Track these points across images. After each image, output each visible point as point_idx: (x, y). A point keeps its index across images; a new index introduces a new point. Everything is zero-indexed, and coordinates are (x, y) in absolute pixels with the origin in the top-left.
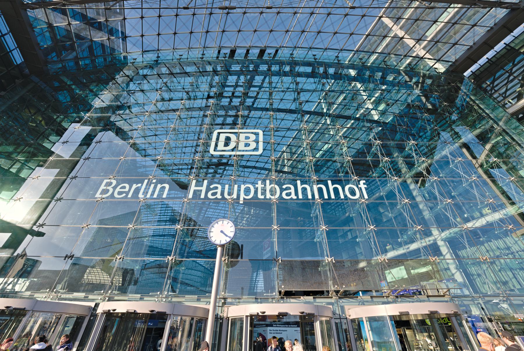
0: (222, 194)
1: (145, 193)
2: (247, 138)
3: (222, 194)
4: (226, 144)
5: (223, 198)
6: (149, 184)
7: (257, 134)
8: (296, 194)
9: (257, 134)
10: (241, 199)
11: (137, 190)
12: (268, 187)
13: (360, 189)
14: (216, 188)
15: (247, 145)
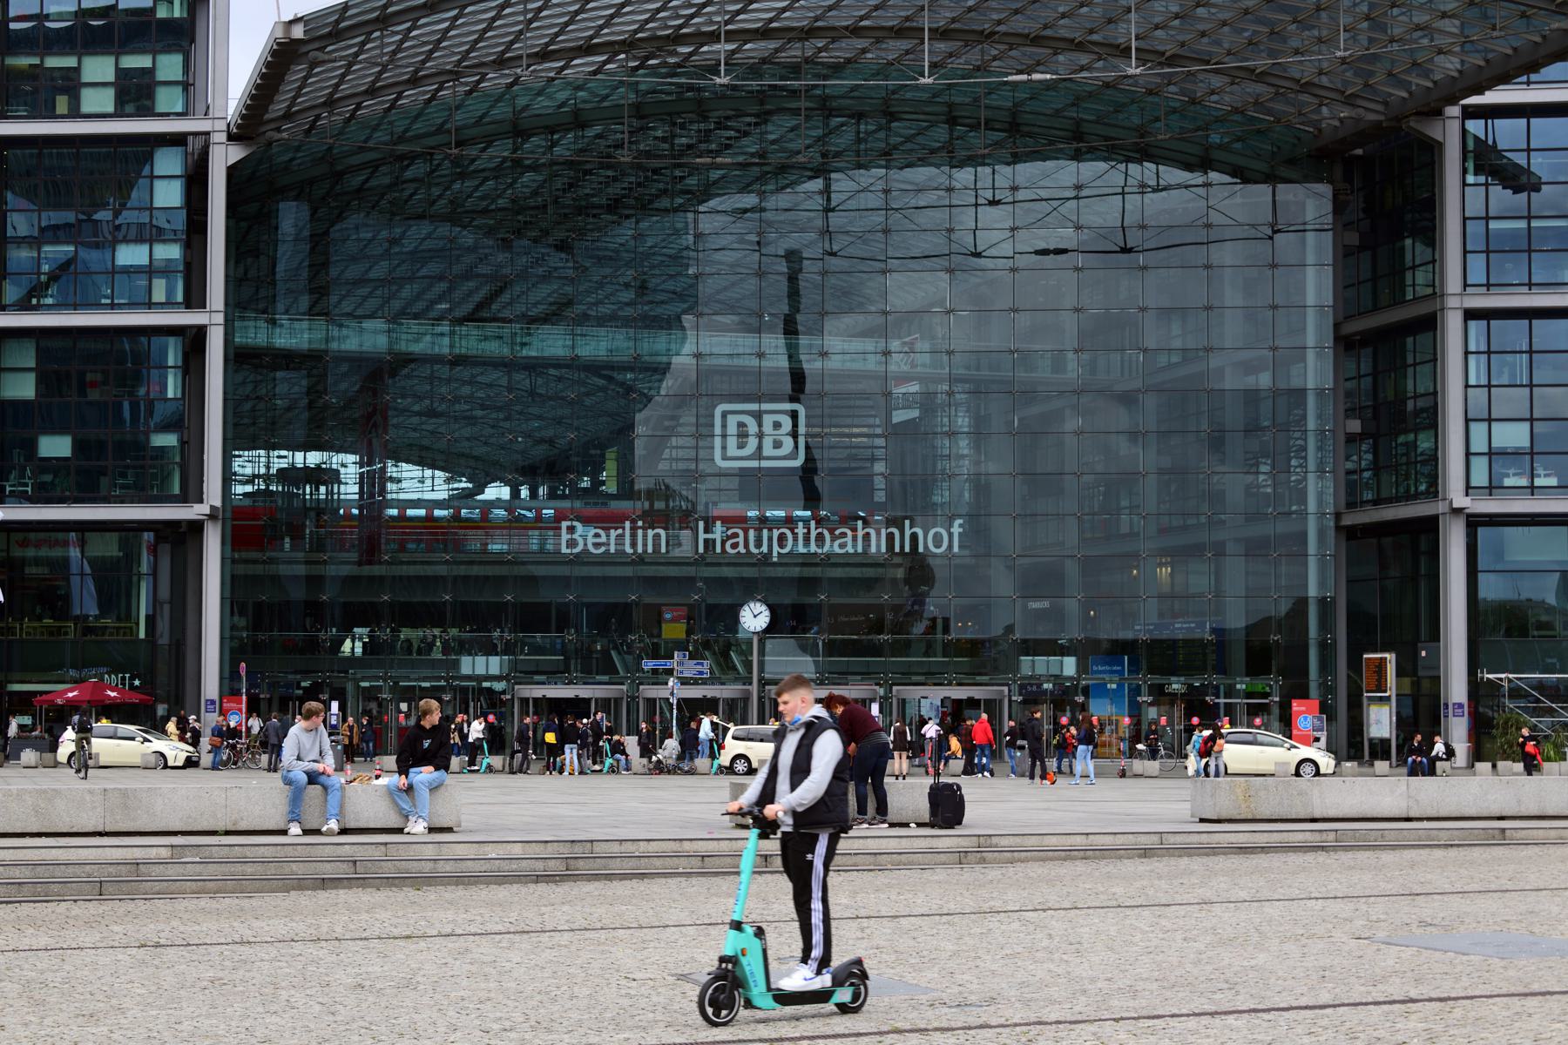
0: (746, 545)
1: (634, 544)
2: (777, 425)
3: (746, 545)
4: (741, 446)
5: (748, 551)
6: (634, 529)
7: (794, 415)
8: (855, 546)
9: (794, 415)
10: (775, 554)
11: (622, 536)
12: (813, 534)
13: (951, 535)
14: (736, 535)
15: (777, 445)
